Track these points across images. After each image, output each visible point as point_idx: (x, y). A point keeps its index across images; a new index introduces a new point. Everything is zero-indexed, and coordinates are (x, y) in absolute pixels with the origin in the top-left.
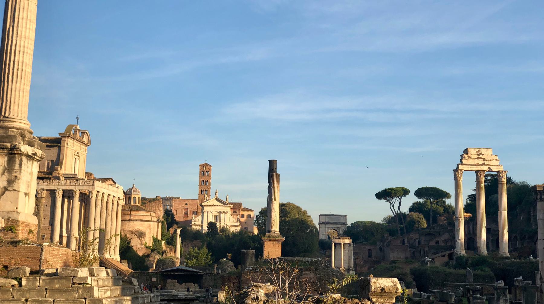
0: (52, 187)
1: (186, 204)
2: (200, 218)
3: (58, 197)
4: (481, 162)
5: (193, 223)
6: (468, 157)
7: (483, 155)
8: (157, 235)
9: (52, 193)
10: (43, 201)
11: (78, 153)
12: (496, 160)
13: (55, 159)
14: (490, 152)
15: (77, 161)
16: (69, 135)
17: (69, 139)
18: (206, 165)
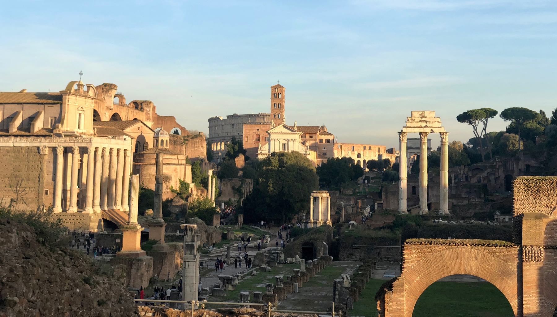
0: (53, 145)
1: (258, 130)
2: (267, 146)
3: (59, 154)
4: (423, 124)
5: (259, 152)
6: (412, 119)
7: (426, 117)
8: (184, 178)
9: (54, 150)
10: (46, 158)
11: (82, 108)
12: (438, 122)
13: (57, 116)
14: (433, 115)
15: (82, 116)
16: (70, 92)
17: (70, 97)
18: (279, 86)
